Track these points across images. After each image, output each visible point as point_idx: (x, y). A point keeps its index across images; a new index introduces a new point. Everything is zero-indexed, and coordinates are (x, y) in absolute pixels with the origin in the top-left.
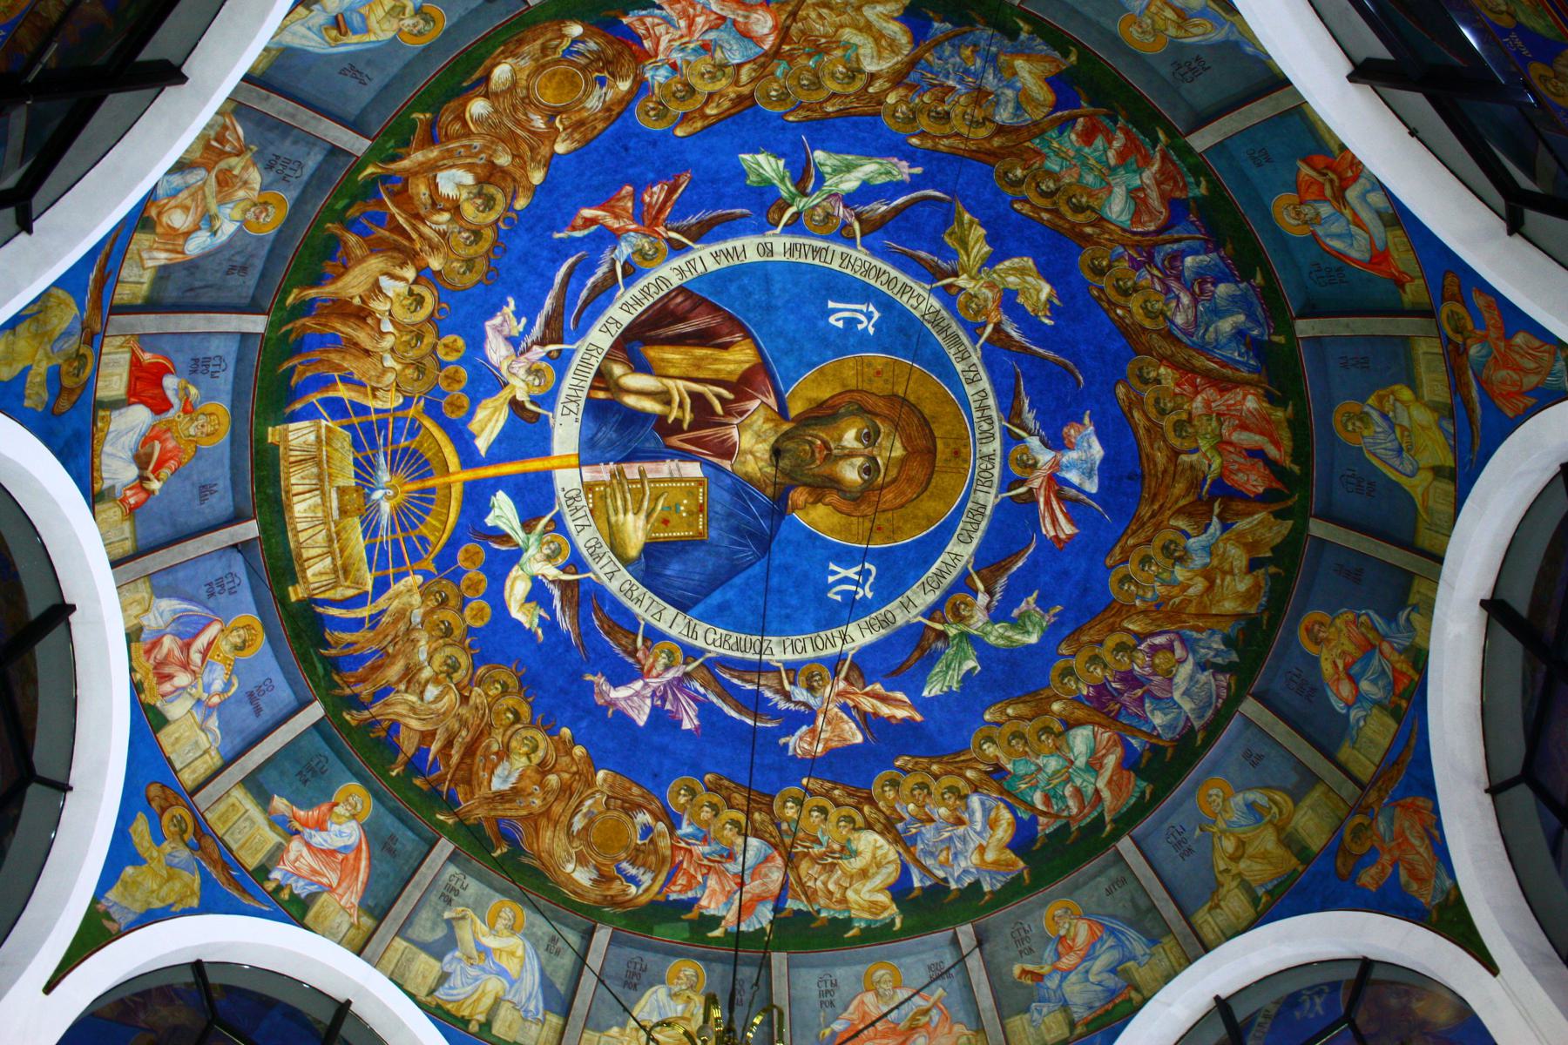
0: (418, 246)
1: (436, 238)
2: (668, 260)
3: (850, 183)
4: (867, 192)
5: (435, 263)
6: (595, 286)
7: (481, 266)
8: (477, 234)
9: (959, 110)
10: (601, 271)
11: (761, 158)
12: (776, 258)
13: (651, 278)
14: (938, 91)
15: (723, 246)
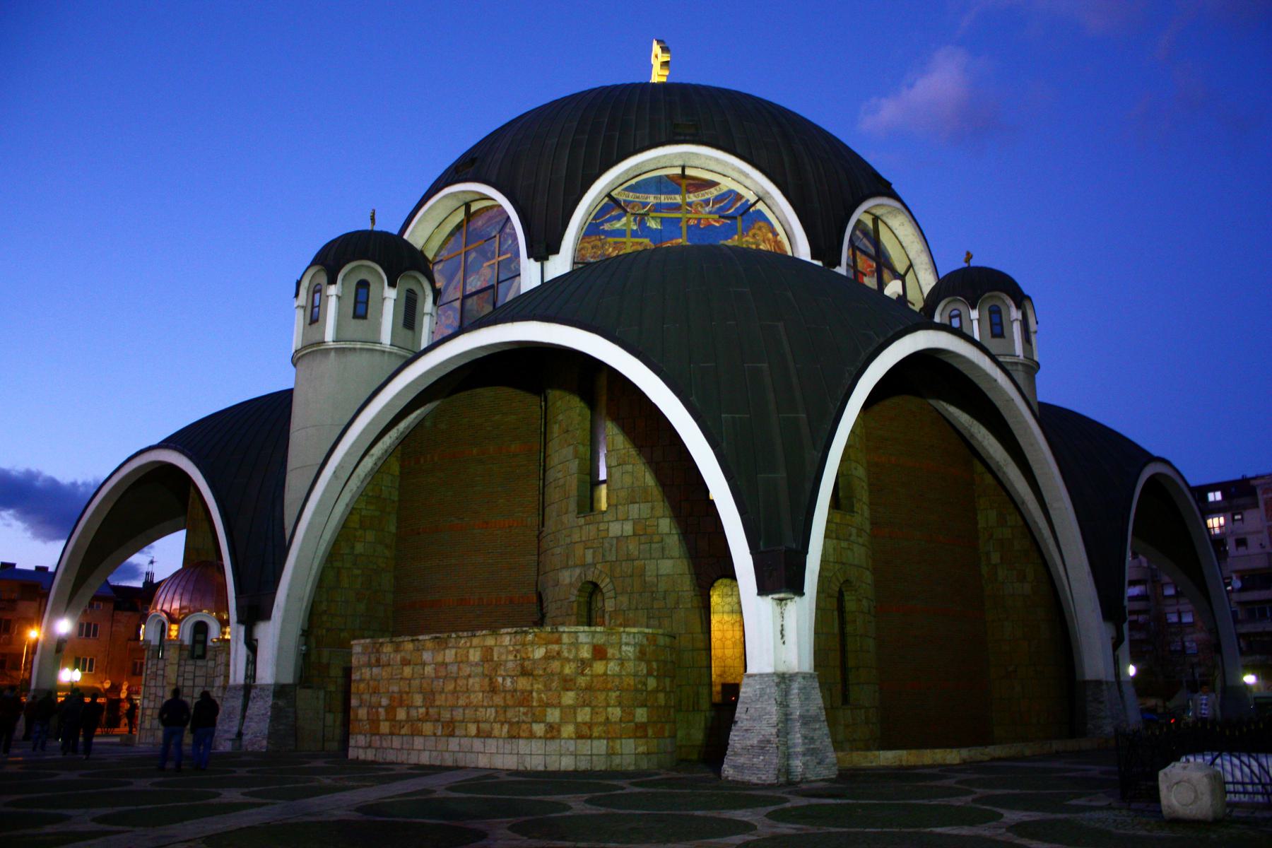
0: (773, 244)
1: (767, 242)
2: (693, 202)
3: (624, 220)
4: (618, 218)
5: (770, 235)
6: (721, 203)
7: (757, 226)
8: (754, 236)
9: (589, 251)
10: (718, 206)
11: (655, 227)
12: (653, 196)
13: (700, 198)
14: (596, 256)
15: (672, 201)
